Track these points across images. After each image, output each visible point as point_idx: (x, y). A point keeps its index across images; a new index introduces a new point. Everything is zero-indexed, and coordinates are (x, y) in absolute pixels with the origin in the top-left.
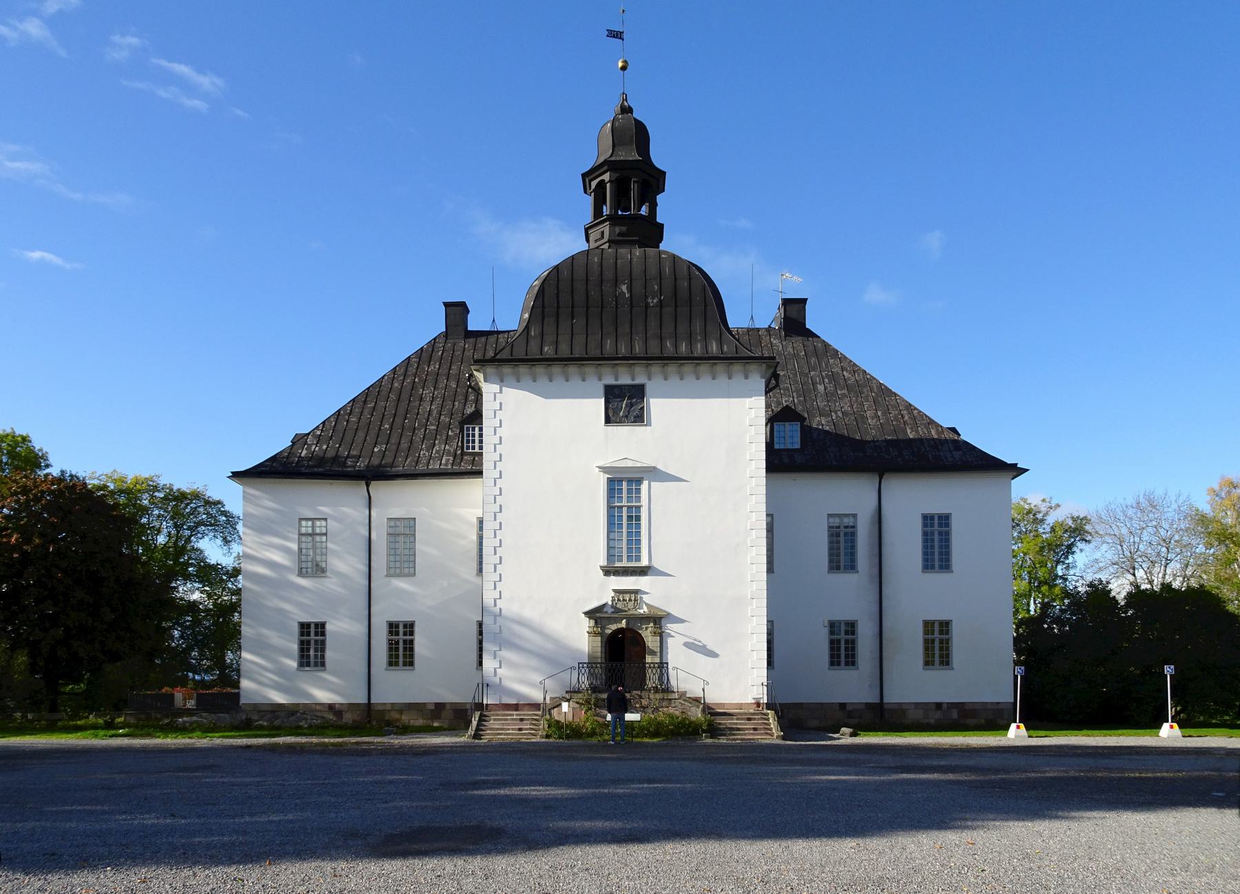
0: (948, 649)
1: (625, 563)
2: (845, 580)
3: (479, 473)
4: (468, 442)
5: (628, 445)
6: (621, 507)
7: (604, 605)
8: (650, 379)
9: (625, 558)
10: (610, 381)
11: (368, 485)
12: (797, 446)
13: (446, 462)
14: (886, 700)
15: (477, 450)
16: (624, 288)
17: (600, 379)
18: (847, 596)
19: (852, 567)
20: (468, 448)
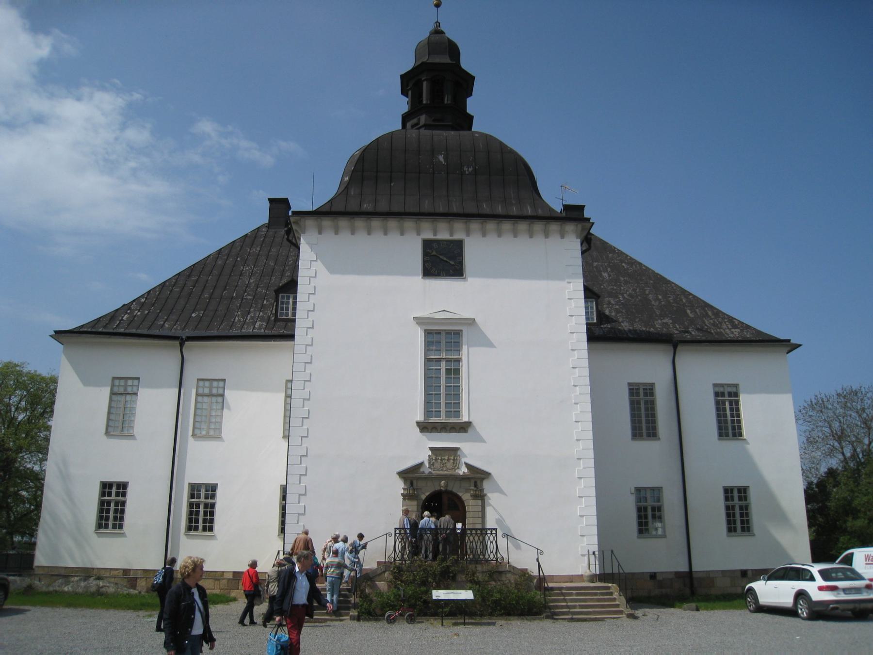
0: (747, 514)
1: (443, 419)
2: (646, 446)
3: (291, 337)
4: (282, 309)
5: (445, 298)
6: (439, 360)
7: (422, 464)
8: (468, 234)
9: (443, 414)
10: (429, 236)
11: (182, 345)
12: (595, 321)
13: (259, 327)
14: (694, 569)
15: (290, 316)
16: (441, 158)
17: (418, 234)
18: (650, 464)
19: (652, 434)
20: (282, 314)
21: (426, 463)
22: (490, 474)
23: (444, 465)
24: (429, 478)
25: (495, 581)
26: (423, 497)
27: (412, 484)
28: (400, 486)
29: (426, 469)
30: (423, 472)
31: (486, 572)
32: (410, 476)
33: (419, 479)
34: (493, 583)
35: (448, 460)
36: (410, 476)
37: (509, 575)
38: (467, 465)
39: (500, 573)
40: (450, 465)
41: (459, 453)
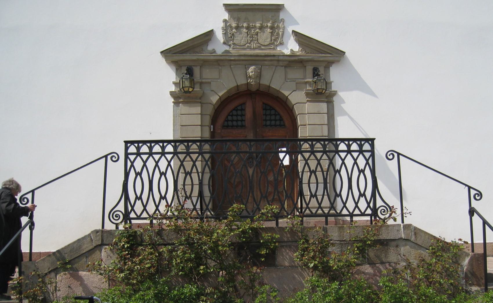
21: (219, 35)
22: (342, 53)
23: (254, 38)
24: (221, 62)
25: (372, 264)
26: (215, 99)
27: (190, 72)
28: (168, 77)
29: (219, 46)
30: (214, 51)
31: (351, 243)
32: (188, 58)
33: (205, 63)
34: (368, 269)
35: (261, 28)
36: (188, 58)
37: (404, 250)
38: (300, 37)
39: (385, 243)
40: (265, 37)
41: (282, 15)
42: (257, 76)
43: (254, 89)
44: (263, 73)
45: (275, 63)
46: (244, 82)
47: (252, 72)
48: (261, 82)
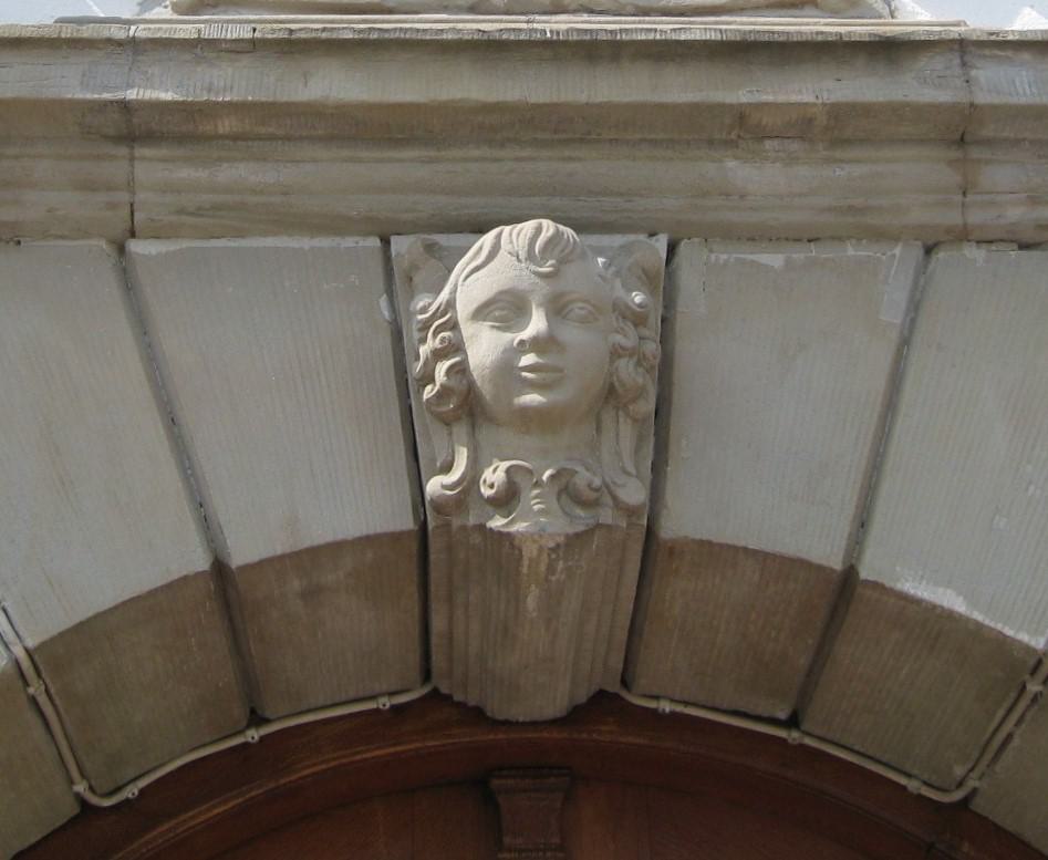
42: (611, 395)
43: (536, 669)
44: (688, 349)
45: (911, 179)
46: (356, 503)
47: (505, 308)
48: (684, 520)
